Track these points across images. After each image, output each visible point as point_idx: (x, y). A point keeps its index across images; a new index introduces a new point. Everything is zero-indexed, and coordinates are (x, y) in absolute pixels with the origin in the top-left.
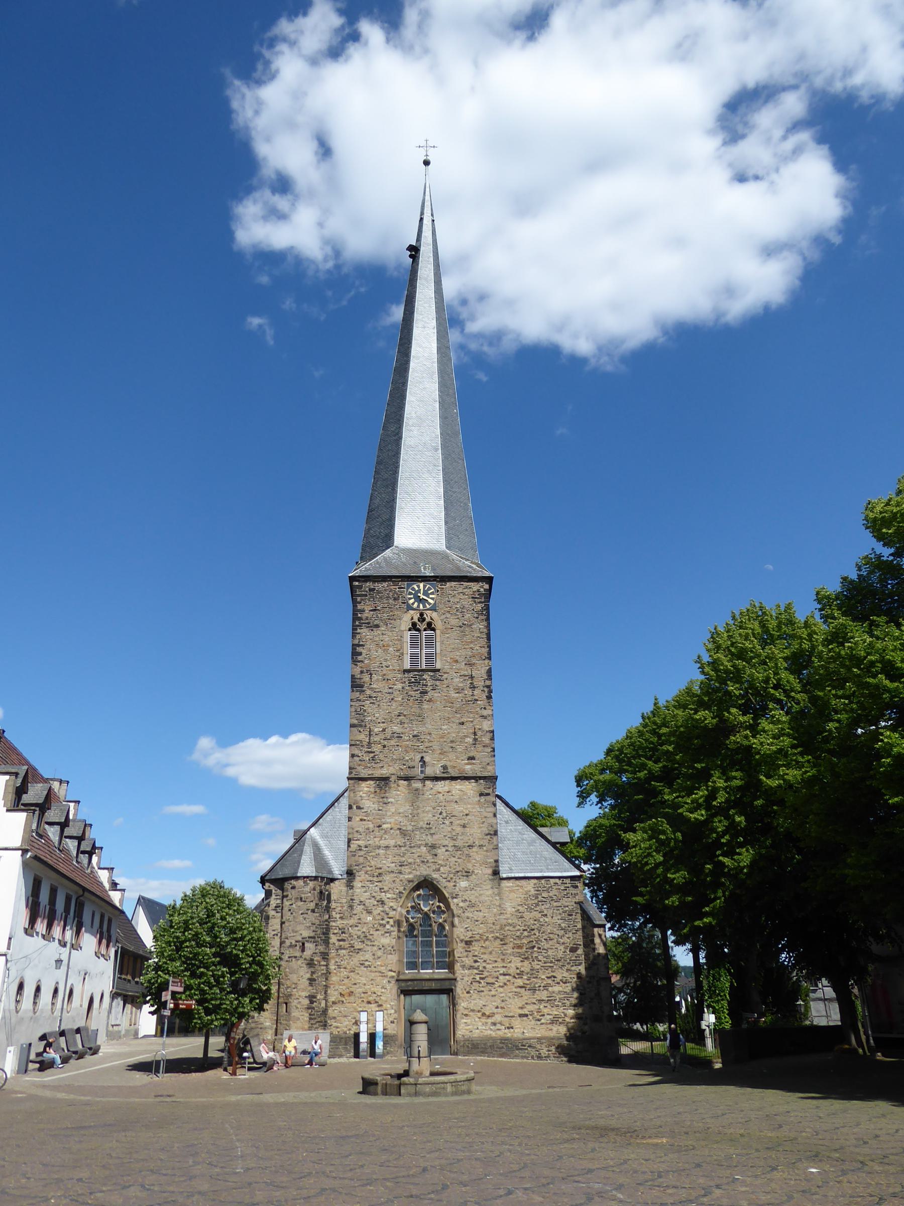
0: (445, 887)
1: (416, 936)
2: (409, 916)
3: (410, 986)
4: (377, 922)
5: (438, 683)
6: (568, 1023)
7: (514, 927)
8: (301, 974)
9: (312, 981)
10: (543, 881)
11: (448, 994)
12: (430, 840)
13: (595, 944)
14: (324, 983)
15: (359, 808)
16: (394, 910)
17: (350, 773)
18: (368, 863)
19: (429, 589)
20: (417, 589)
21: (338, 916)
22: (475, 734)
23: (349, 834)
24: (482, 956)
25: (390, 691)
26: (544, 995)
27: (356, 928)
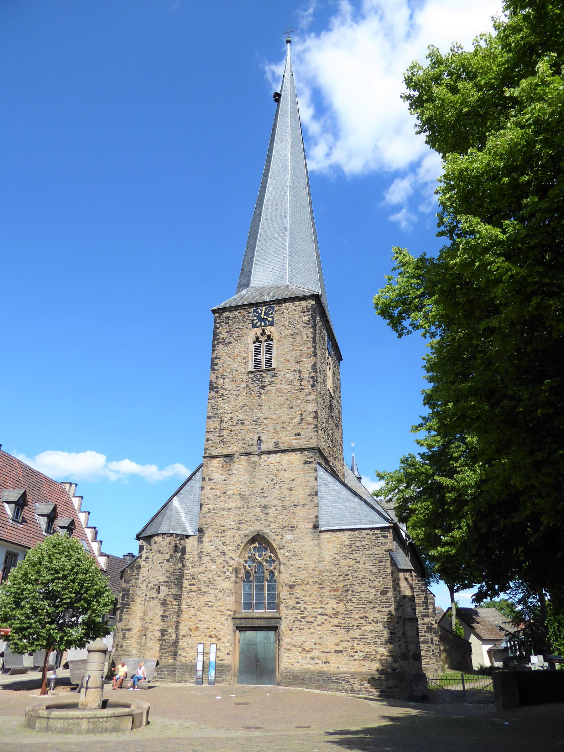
0: (274, 540)
1: (251, 582)
2: (247, 565)
3: (244, 623)
4: (219, 570)
5: (273, 379)
6: (381, 660)
7: (331, 573)
8: (156, 611)
9: (164, 617)
10: (356, 532)
11: (275, 631)
12: (263, 502)
13: (400, 588)
14: (176, 620)
15: (210, 479)
16: (233, 559)
17: (206, 453)
18: (215, 523)
19: (269, 311)
20: (260, 312)
21: (191, 565)
22: (301, 415)
23: (201, 500)
24: (303, 598)
25: (237, 389)
26: (356, 633)
27: (204, 575)
